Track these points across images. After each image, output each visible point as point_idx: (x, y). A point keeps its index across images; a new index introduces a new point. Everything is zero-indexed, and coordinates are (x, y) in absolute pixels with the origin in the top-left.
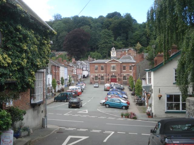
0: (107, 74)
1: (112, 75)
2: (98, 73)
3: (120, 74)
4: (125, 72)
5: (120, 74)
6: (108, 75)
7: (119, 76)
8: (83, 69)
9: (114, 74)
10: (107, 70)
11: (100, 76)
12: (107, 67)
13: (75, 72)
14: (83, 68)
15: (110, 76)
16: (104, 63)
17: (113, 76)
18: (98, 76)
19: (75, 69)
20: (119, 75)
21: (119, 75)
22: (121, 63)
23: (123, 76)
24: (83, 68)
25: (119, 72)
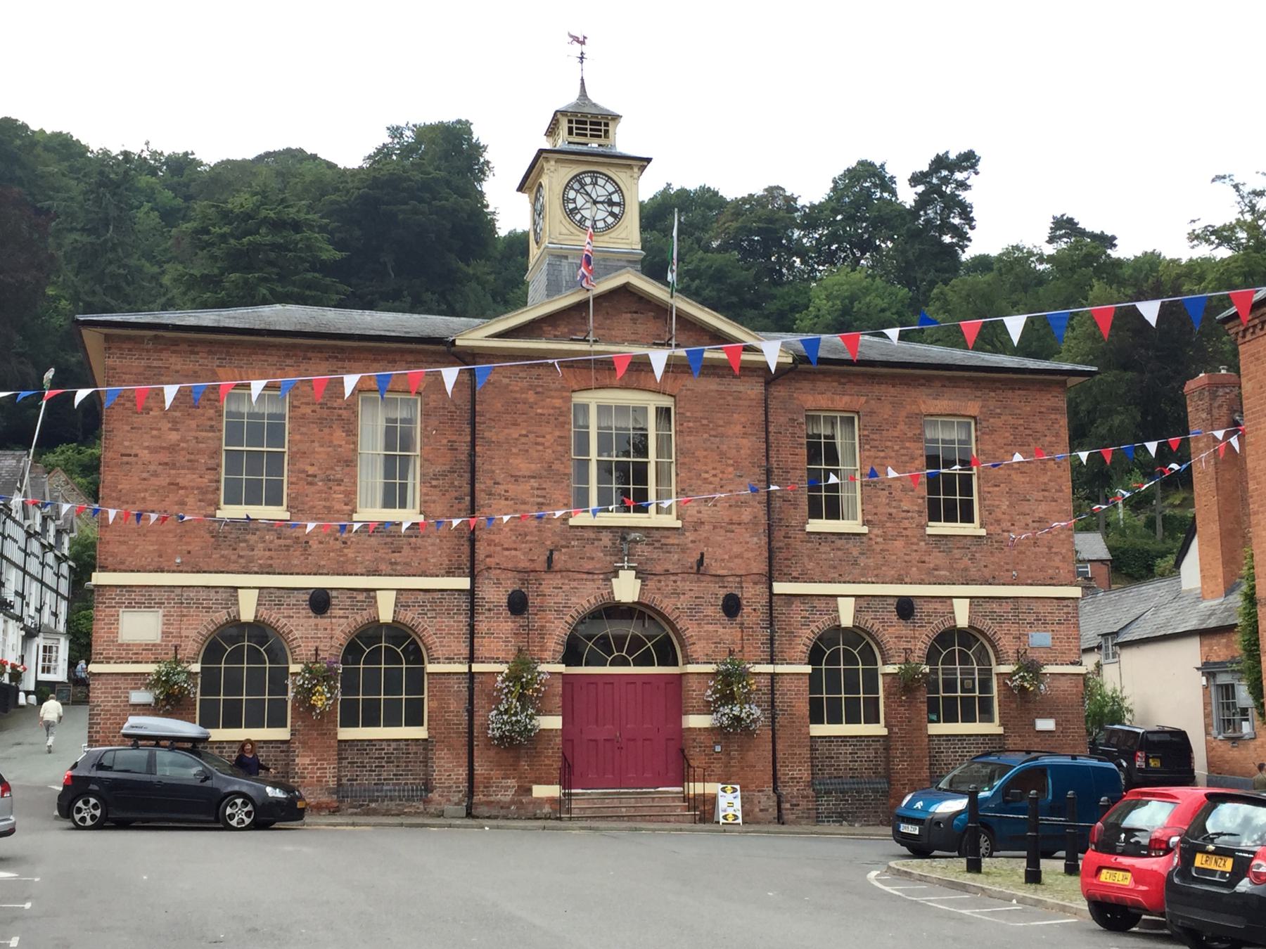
0: (494, 594)
1: (585, 597)
2: (285, 548)
3: (752, 613)
4: (844, 558)
5: (752, 594)
6: (518, 604)
7: (728, 633)
9: (626, 588)
12: (488, 432)
15: (558, 631)
17: (612, 629)
20: (732, 606)
21: (732, 606)
23: (805, 638)
25: (741, 552)
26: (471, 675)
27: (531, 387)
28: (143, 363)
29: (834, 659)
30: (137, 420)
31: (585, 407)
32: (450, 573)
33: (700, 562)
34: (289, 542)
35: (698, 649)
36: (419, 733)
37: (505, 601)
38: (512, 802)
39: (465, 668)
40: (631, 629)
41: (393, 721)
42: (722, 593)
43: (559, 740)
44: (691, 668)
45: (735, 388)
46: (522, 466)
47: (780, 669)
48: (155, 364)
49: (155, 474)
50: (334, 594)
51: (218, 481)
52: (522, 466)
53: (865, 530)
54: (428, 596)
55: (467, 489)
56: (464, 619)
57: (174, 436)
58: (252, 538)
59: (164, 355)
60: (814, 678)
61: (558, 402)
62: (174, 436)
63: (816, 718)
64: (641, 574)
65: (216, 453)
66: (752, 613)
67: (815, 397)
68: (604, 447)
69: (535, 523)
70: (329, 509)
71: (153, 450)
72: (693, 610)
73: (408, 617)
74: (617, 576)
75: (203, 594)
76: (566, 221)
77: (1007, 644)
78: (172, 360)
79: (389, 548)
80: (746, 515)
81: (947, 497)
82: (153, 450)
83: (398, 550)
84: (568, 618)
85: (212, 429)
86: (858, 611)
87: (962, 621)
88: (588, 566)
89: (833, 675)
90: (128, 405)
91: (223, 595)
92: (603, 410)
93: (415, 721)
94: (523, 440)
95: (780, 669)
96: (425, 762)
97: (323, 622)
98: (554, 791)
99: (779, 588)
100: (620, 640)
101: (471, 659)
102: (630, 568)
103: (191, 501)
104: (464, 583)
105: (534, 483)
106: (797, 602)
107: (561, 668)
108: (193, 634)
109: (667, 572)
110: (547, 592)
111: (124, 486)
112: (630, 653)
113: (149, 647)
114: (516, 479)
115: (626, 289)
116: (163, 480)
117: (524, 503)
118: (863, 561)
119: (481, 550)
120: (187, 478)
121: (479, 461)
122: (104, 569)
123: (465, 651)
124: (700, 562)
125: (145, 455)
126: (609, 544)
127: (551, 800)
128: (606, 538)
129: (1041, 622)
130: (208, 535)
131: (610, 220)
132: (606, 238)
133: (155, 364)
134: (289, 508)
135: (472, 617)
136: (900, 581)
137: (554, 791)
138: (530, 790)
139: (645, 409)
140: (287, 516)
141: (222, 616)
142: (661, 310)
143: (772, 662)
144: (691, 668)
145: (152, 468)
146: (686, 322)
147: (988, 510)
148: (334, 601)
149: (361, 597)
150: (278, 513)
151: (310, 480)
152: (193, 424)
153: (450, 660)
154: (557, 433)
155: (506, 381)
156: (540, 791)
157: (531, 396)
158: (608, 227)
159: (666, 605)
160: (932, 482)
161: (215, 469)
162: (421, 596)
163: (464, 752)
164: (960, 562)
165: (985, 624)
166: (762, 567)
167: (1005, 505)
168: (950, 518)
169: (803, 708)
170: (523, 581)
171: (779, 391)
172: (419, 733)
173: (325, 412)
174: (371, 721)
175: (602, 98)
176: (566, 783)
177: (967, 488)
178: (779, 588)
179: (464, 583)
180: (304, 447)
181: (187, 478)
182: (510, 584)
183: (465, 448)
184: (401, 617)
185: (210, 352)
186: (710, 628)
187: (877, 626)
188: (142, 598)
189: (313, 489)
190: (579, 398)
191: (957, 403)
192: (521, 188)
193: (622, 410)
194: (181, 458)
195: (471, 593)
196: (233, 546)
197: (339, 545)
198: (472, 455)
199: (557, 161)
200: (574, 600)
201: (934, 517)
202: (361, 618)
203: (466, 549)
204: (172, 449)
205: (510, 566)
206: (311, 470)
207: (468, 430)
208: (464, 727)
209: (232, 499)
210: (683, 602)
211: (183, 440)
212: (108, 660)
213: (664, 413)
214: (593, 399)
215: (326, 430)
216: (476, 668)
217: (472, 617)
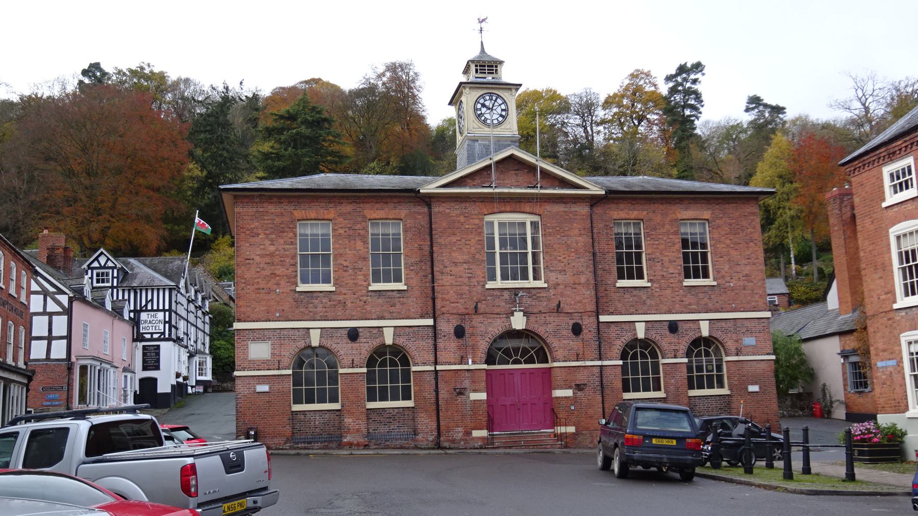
0: (447, 327)
1: (496, 328)
2: (333, 306)
3: (589, 331)
4: (638, 302)
5: (588, 323)
6: (459, 332)
7: (575, 344)
8: (135, 322)
9: (518, 322)
10: (444, 281)
11: (365, 347)
12: (439, 240)
13: (50, 338)
14: (137, 312)
15: (483, 346)
16: (412, 195)
17: (511, 344)
18: (328, 343)
19: (52, 307)
20: (577, 330)
21: (577, 330)
22: (594, 201)
23: (618, 346)
24: (137, 312)
26: (436, 372)
27: (462, 214)
28: (254, 209)
29: (634, 357)
30: (252, 240)
31: (492, 223)
32: (422, 317)
33: (559, 306)
34: (334, 303)
35: (559, 354)
36: (409, 404)
37: (452, 331)
38: (461, 440)
39: (432, 368)
40: (522, 344)
41: (395, 398)
42: (571, 322)
43: (485, 405)
44: (556, 364)
45: (573, 209)
46: (459, 257)
47: (606, 363)
48: (261, 210)
49: (263, 269)
50: (360, 330)
51: (296, 272)
52: (459, 257)
53: (649, 285)
54: (411, 329)
55: (429, 270)
56: (431, 342)
57: (272, 248)
58: (316, 302)
59: (265, 205)
60: (624, 368)
61: (477, 221)
62: (272, 248)
63: (626, 389)
64: (526, 314)
65: (294, 257)
66: (589, 331)
67: (617, 212)
68: (503, 244)
69: (467, 288)
70: (356, 284)
71: (262, 256)
72: (556, 333)
73: (401, 341)
74: (513, 315)
75: (291, 332)
76: (476, 121)
77: (731, 345)
78: (270, 207)
79: (391, 305)
80: (583, 279)
81: (695, 264)
82: (262, 256)
83: (393, 305)
84: (487, 339)
85: (292, 243)
86: (647, 330)
87: (705, 333)
88: (497, 310)
89: (634, 365)
90: (248, 232)
91: (303, 332)
92: (502, 225)
93: (407, 397)
94: (459, 243)
95: (606, 363)
96: (413, 419)
97: (355, 345)
98: (484, 433)
99: (603, 318)
100: (516, 350)
101: (436, 363)
102: (520, 311)
103: (282, 283)
104: (430, 322)
105: (466, 266)
106: (613, 326)
107: (485, 366)
108: (287, 354)
109: (540, 312)
110: (476, 325)
111: (247, 275)
112: (522, 357)
113: (265, 362)
114: (456, 264)
115: (511, 157)
116: (267, 272)
117: (461, 277)
118: (648, 302)
119: (439, 304)
120: (280, 271)
121: (435, 255)
122: (239, 321)
123: (432, 359)
124: (559, 306)
125: (257, 259)
126: (508, 298)
127: (482, 438)
128: (506, 295)
129: (749, 332)
130: (292, 301)
131: (501, 119)
132: (499, 129)
133: (261, 210)
134: (335, 285)
135: (435, 340)
136: (669, 312)
137: (484, 433)
138: (471, 433)
139: (524, 224)
140: (333, 289)
141: (302, 344)
142: (532, 168)
143: (600, 359)
144: (556, 364)
145: (262, 266)
146: (545, 174)
147: (717, 271)
148: (361, 334)
149: (375, 331)
150: (329, 287)
151: (345, 269)
152: (282, 241)
153: (424, 364)
154: (477, 238)
155: (448, 211)
156: (476, 433)
157: (462, 219)
158: (500, 123)
159: (541, 330)
160: (685, 255)
161: (295, 265)
162: (407, 330)
163: (434, 413)
164: (703, 301)
165: (718, 334)
166: (591, 307)
167: (726, 267)
168: (696, 276)
169: (619, 385)
170: (462, 320)
171: (598, 210)
172: (409, 404)
173: (351, 232)
174: (383, 398)
175: (493, 52)
176: (490, 428)
177: (705, 260)
178: (603, 318)
179: (430, 322)
180: (341, 251)
181: (280, 271)
182: (455, 322)
183: (427, 248)
184: (397, 342)
185: (289, 202)
186: (566, 342)
187: (658, 337)
188: (259, 336)
189: (346, 274)
190: (488, 218)
191: (698, 212)
192: (450, 104)
193: (512, 224)
194: (276, 260)
195: (434, 327)
196: (306, 305)
197: (362, 303)
198: (432, 253)
199: (470, 88)
200: (490, 329)
201: (687, 276)
202: (376, 343)
203: (430, 303)
204: (271, 255)
205: (455, 311)
206: (345, 264)
207: (429, 239)
208: (433, 400)
209: (305, 281)
210: (550, 328)
211: (277, 250)
212: (244, 369)
213: (534, 225)
214: (496, 219)
215: (353, 242)
216: (439, 368)
217: (435, 340)
